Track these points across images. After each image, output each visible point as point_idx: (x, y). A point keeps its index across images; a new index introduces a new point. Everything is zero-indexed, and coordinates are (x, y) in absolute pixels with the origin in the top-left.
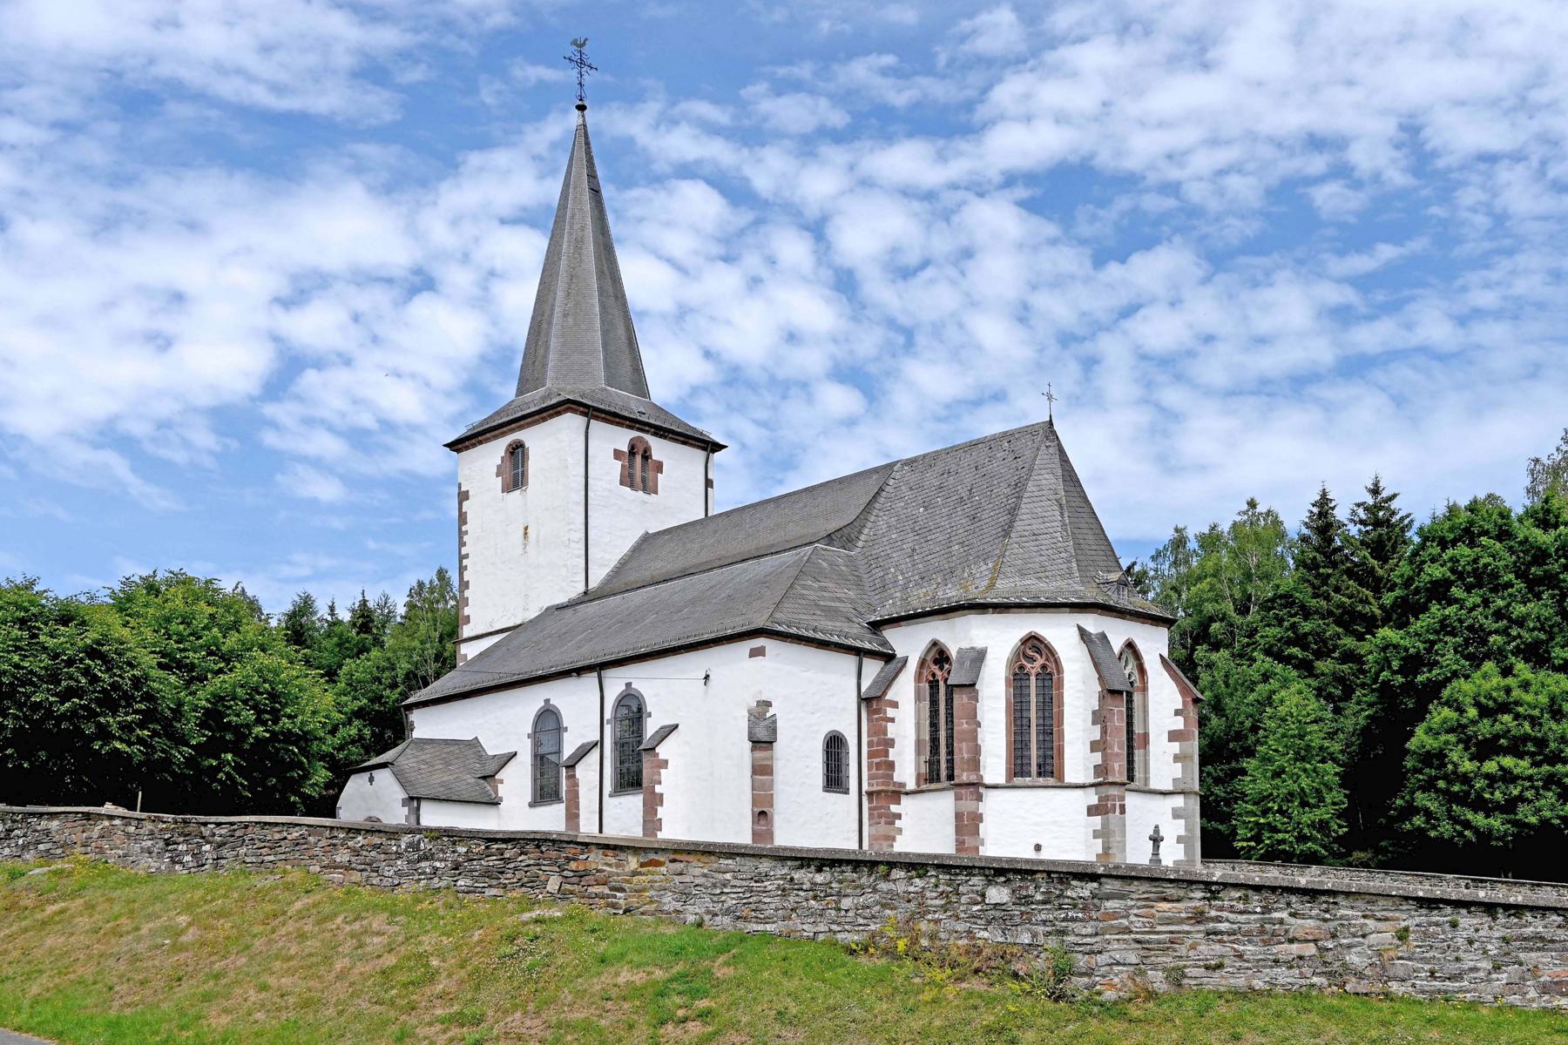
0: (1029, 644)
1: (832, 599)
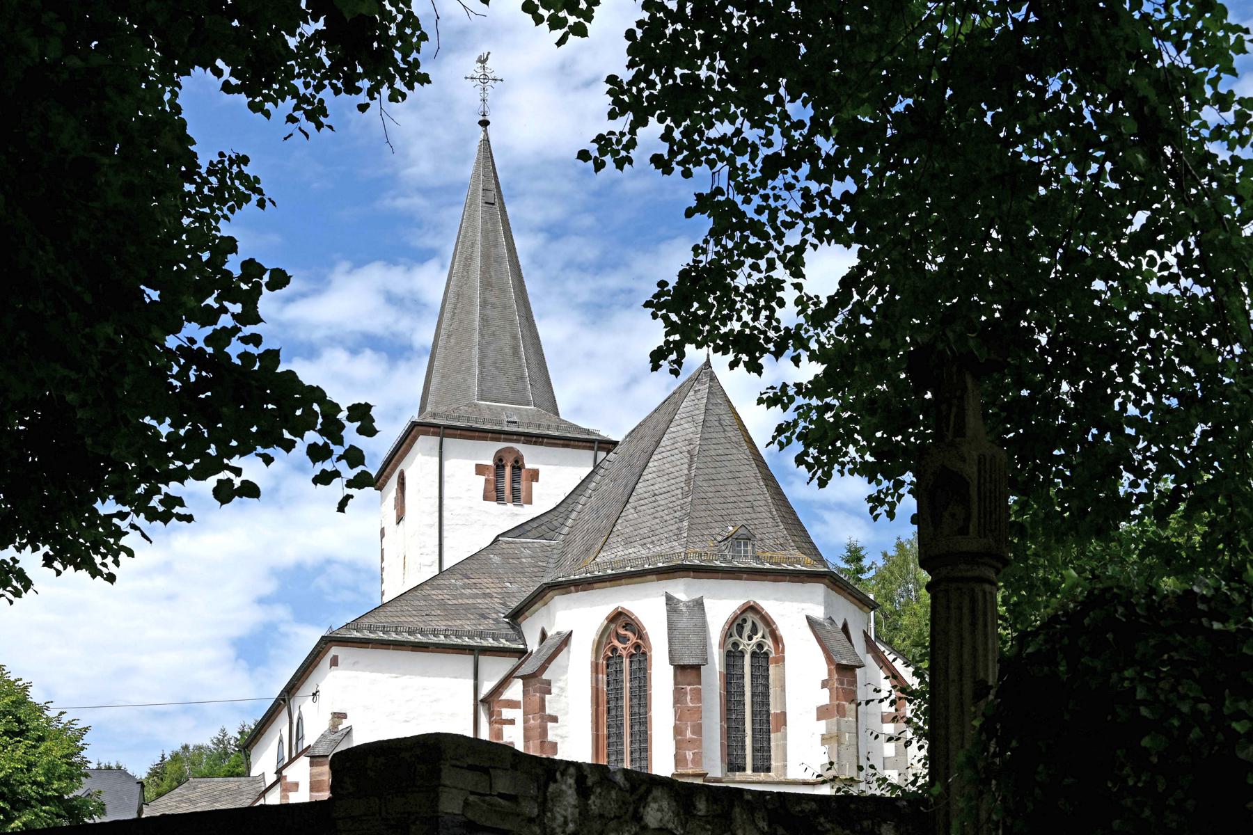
0: (621, 621)
1: (475, 596)
